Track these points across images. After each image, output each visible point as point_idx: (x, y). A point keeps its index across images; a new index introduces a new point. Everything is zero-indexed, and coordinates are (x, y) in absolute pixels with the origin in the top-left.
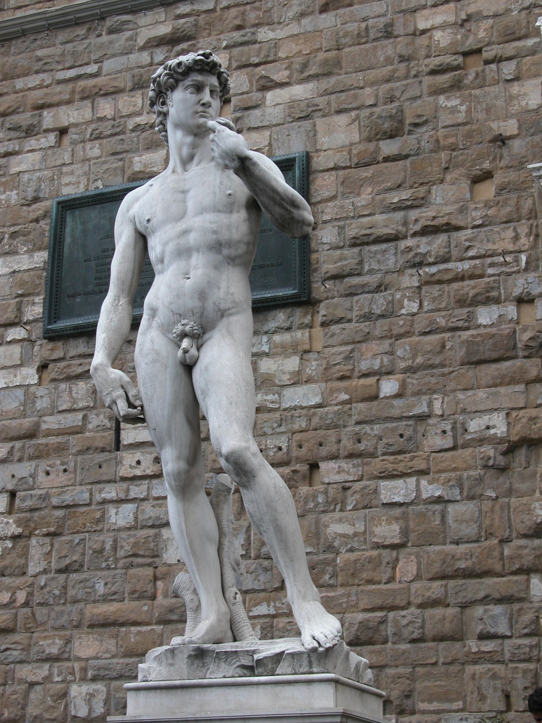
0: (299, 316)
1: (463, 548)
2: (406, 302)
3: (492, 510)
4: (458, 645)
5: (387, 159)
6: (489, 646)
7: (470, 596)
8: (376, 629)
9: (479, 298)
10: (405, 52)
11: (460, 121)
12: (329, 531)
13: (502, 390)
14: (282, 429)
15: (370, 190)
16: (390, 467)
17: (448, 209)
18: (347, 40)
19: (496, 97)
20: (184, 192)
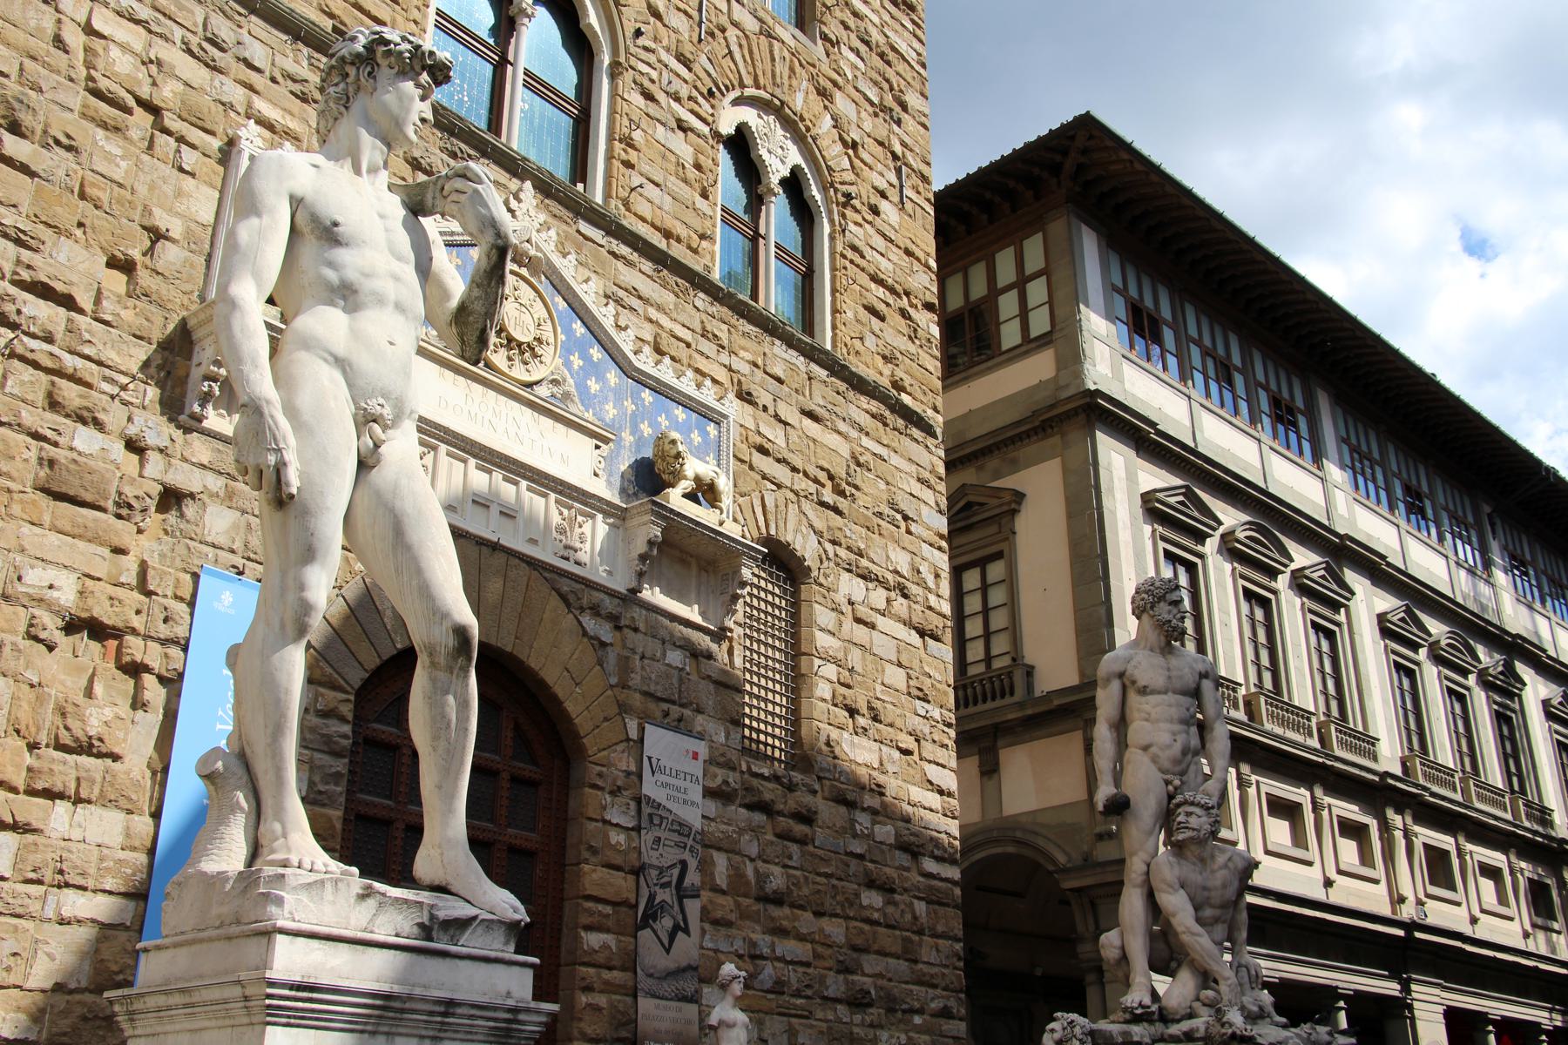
9: (86, 414)
11: (116, 177)
13: (81, 544)
17: (75, 278)
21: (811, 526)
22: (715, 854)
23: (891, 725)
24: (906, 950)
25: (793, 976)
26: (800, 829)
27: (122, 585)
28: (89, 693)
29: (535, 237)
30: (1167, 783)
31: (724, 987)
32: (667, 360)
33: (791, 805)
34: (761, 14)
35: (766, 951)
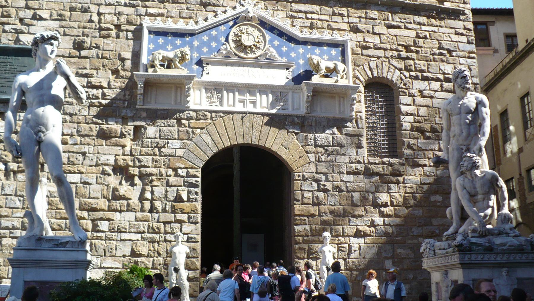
21: (396, 68)
28: (120, 184)
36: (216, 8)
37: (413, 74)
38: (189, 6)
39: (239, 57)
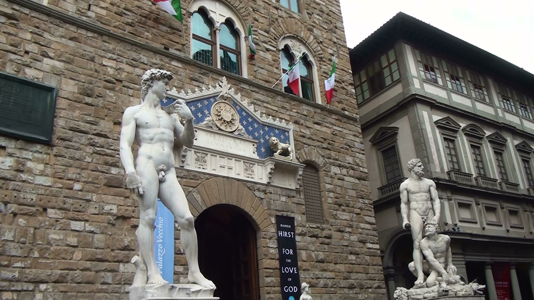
0: (44, 149)
1: (99, 251)
2: (87, 157)
3: (109, 239)
4: (93, 285)
5: (86, 104)
6: (105, 287)
7: (99, 268)
8: (65, 277)
9: (113, 164)
10: (98, 69)
12: (50, 236)
13: (117, 197)
14: (34, 192)
15: (79, 112)
16: (76, 216)
17: (106, 130)
18: (77, 54)
19: (125, 99)
20: (158, 117)
22: (302, 251)
23: (352, 207)
24: (365, 271)
25: (330, 282)
26: (327, 241)
27: (128, 206)
29: (228, 92)
30: (423, 218)
31: (304, 289)
32: (271, 117)
33: (324, 235)
34: (288, 12)
35: (320, 276)
36: (200, 85)
37: (331, 161)
38: (179, 77)
39: (220, 129)
